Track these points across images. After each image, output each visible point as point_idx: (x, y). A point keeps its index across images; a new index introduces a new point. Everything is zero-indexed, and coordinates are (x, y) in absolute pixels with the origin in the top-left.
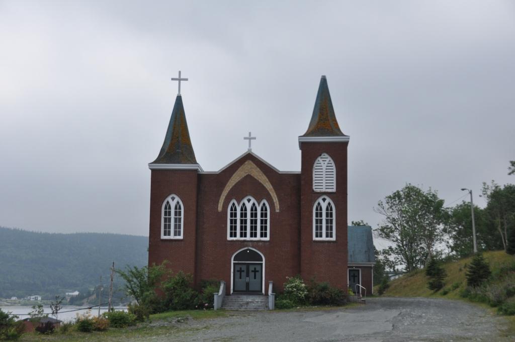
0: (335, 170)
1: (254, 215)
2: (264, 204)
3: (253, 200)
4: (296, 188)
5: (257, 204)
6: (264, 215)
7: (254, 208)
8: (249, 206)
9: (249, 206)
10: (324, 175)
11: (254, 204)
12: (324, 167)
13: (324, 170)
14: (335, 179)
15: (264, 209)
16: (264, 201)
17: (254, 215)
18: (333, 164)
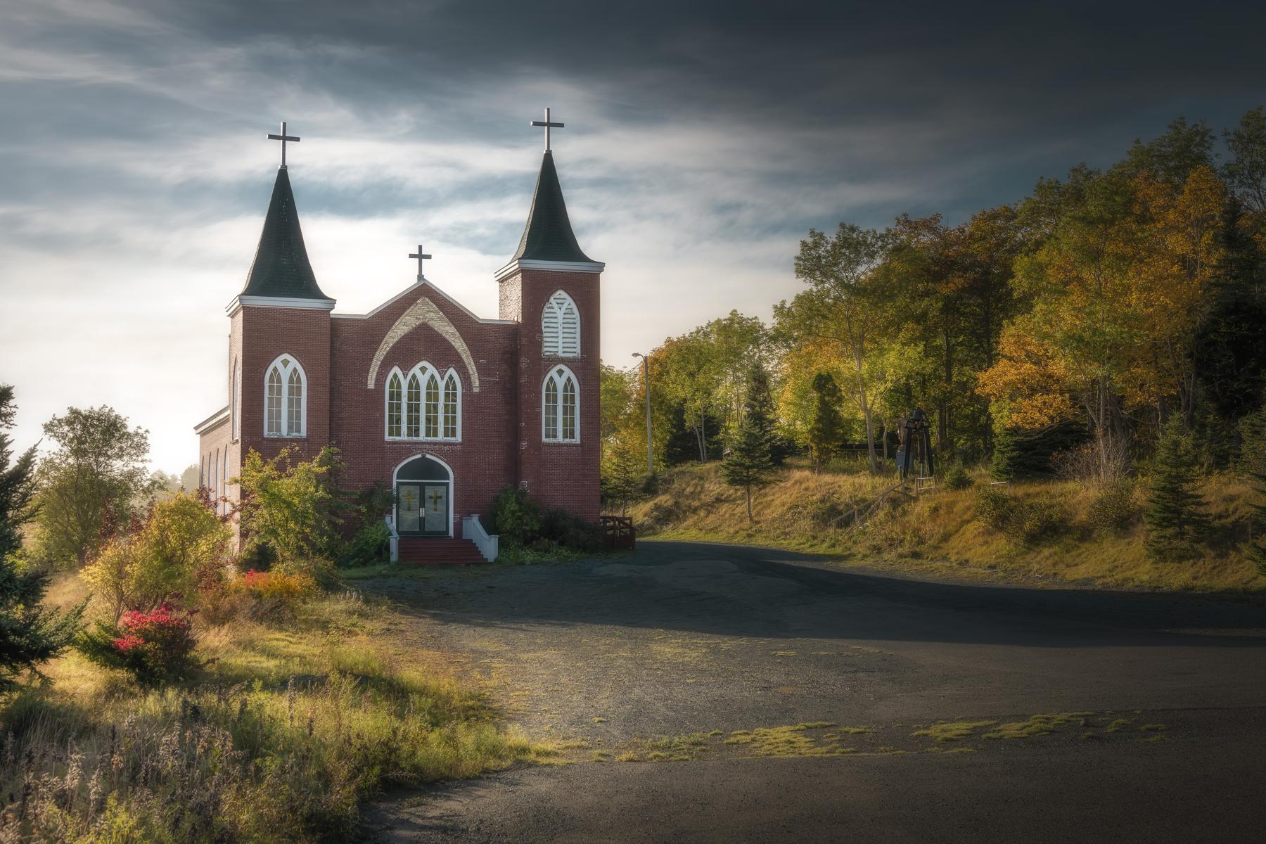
0: (578, 320)
1: (432, 396)
2: (451, 378)
3: (431, 369)
4: (509, 354)
5: (438, 377)
6: (450, 396)
7: (432, 382)
8: (423, 380)
9: (423, 380)
10: (559, 324)
11: (432, 377)
12: (560, 314)
13: (560, 320)
14: (578, 335)
15: (450, 384)
16: (452, 371)
17: (432, 396)
18: (576, 310)
